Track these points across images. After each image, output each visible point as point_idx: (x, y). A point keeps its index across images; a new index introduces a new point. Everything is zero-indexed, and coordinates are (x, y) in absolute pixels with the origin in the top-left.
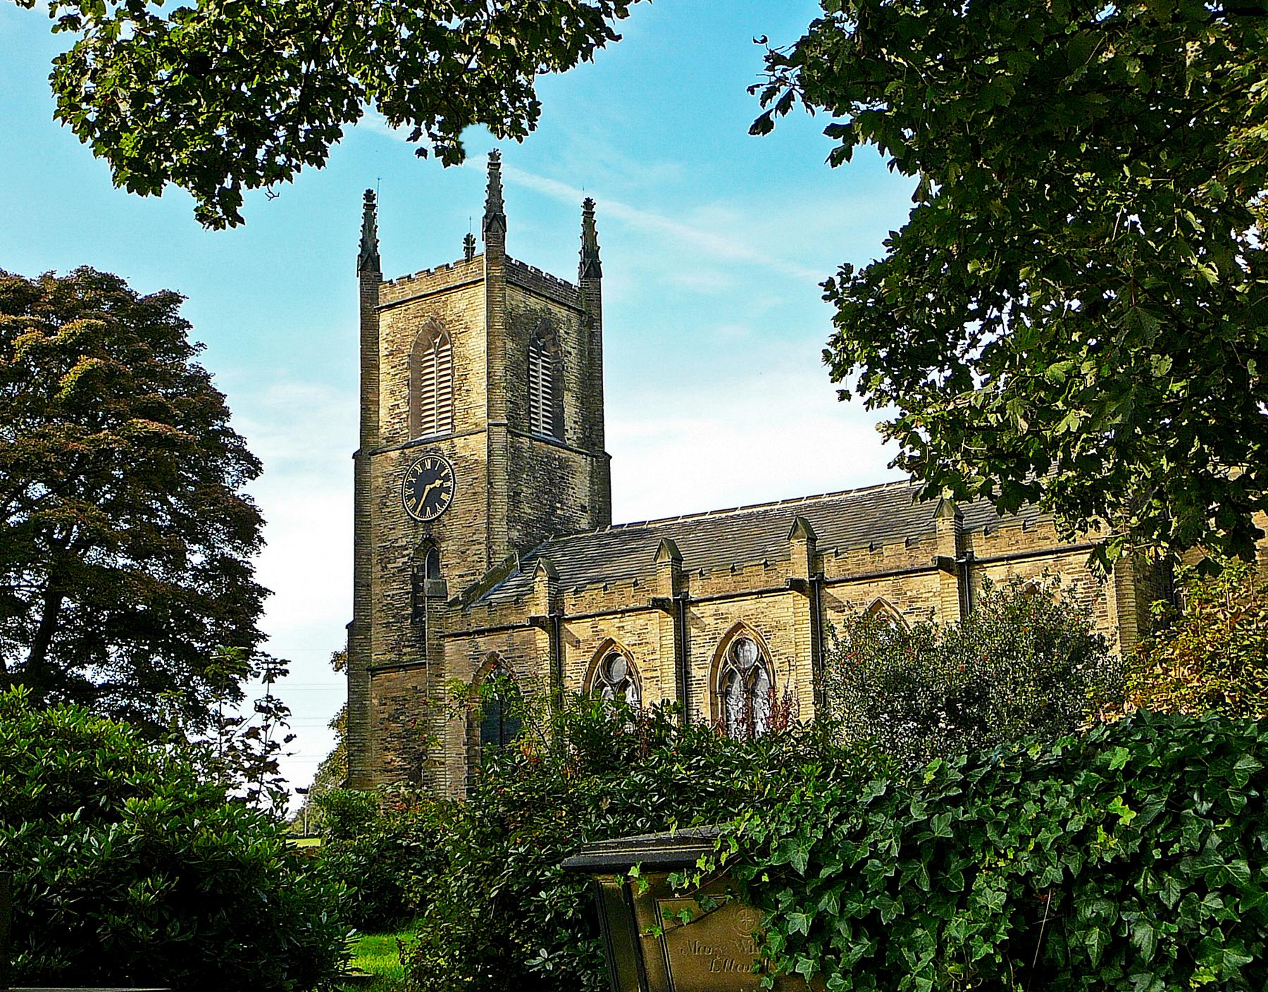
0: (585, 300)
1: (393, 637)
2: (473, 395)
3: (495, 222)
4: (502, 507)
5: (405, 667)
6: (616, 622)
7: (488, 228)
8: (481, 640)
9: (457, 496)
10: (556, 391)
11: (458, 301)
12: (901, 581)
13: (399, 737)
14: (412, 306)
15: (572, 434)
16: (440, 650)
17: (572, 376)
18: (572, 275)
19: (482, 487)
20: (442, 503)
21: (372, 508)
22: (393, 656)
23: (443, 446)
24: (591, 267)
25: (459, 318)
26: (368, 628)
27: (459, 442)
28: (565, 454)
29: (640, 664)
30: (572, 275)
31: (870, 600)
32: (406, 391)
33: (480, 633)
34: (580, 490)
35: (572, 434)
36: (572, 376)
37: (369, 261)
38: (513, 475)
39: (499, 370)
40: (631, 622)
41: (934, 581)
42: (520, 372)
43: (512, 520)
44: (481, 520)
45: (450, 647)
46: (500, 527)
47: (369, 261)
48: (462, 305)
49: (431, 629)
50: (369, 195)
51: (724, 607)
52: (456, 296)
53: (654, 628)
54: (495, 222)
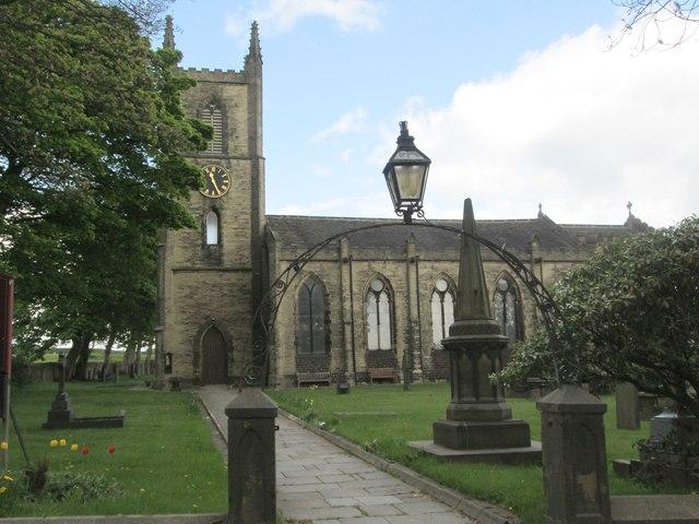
1: (189, 254)
2: (241, 139)
5: (198, 270)
13: (192, 306)
22: (185, 264)
23: (223, 161)
26: (172, 248)
27: (234, 162)
29: (394, 285)
44: (247, 203)
51: (436, 265)
52: (228, 87)
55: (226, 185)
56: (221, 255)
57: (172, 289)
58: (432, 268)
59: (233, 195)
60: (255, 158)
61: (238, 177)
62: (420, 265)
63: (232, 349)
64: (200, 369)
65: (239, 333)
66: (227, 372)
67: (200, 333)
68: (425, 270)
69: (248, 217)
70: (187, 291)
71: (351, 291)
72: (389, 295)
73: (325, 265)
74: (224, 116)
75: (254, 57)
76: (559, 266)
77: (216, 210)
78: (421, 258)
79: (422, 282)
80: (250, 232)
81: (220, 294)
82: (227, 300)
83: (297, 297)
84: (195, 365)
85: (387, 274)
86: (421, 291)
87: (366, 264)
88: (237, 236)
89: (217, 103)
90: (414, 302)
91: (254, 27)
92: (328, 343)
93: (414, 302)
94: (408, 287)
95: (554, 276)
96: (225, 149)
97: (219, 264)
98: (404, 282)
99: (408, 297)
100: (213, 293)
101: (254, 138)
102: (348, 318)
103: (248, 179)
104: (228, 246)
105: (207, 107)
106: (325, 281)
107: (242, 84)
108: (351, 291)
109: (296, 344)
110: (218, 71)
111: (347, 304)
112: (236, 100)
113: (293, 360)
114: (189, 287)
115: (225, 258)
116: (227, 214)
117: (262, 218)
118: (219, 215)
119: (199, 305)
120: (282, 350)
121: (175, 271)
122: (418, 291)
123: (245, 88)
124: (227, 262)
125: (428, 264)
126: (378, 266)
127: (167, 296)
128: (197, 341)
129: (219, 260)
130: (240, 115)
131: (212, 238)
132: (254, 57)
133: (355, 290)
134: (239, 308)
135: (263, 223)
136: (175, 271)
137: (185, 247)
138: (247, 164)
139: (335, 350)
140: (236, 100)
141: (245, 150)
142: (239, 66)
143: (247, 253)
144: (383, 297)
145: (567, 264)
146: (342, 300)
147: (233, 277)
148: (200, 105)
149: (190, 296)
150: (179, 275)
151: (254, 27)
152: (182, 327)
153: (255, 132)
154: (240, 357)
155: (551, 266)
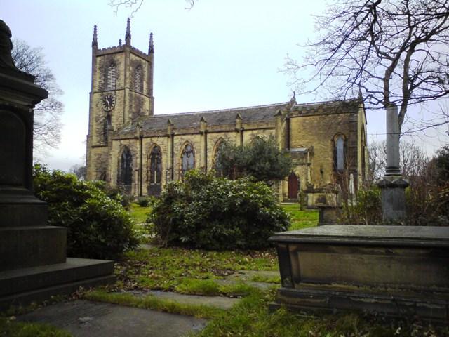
0: (149, 58)
1: (99, 139)
3: (128, 36)
4: (127, 108)
5: (102, 146)
6: (156, 139)
7: (126, 38)
8: (122, 141)
9: (116, 106)
10: (142, 81)
12: (227, 133)
14: (106, 56)
15: (145, 92)
16: (111, 143)
17: (146, 77)
18: (146, 51)
19: (122, 103)
21: (94, 106)
22: (98, 144)
23: (113, 92)
24: (151, 51)
25: (118, 60)
27: (117, 92)
28: (143, 96)
30: (146, 51)
31: (219, 137)
32: (103, 78)
34: (147, 105)
35: (145, 92)
36: (146, 77)
37: (95, 44)
38: (131, 101)
39: (128, 74)
40: (161, 139)
41: (234, 134)
42: (134, 75)
43: (130, 112)
44: (122, 111)
45: (114, 142)
46: (127, 113)
47: (95, 44)
49: (109, 138)
50: (95, 26)
51: (184, 137)
53: (166, 141)
54: (128, 36)
58: (181, 139)
61: (119, 99)
70: (97, 156)
73: (132, 141)
76: (255, 132)
79: (175, 146)
85: (159, 143)
86: (175, 152)
87: (149, 139)
95: (251, 139)
103: (122, 99)
105: (110, 66)
106: (131, 149)
107: (123, 52)
110: (104, 49)
119: (102, 163)
122: (173, 153)
123: (124, 53)
125: (179, 137)
126: (154, 140)
133: (144, 152)
141: (122, 85)
145: (260, 131)
149: (98, 159)
150: (95, 149)
155: (250, 132)
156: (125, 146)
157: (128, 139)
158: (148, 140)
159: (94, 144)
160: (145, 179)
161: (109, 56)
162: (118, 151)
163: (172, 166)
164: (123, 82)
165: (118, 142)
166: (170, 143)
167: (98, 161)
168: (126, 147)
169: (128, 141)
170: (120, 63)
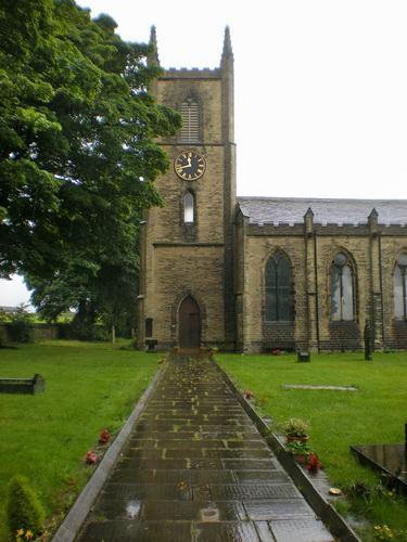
2: (214, 128)
5: (176, 245)
6: (345, 240)
8: (270, 240)
9: (207, 171)
11: (207, 86)
13: (170, 277)
20: (198, 174)
22: (165, 240)
23: (199, 148)
27: (208, 148)
29: (356, 258)
33: (270, 236)
40: (351, 241)
44: (221, 185)
48: (208, 88)
52: (204, 83)
55: (201, 169)
56: (197, 231)
57: (153, 261)
58: (395, 243)
59: (208, 177)
60: (227, 145)
61: (213, 161)
62: (382, 240)
63: (205, 316)
64: (177, 333)
65: (212, 303)
66: (200, 337)
67: (177, 301)
68: (388, 245)
69: (221, 197)
70: (167, 263)
71: (315, 264)
72: (352, 269)
74: (200, 108)
75: (227, 55)
77: (192, 191)
78: (383, 233)
79: (384, 256)
80: (221, 210)
81: (197, 268)
82: (201, 271)
83: (264, 269)
84: (173, 330)
86: (383, 264)
87: (330, 238)
88: (210, 214)
89: (194, 97)
90: (376, 275)
91: (227, 31)
92: (292, 313)
93: (376, 275)
94: (371, 265)
96: (201, 137)
97: (194, 240)
98: (366, 256)
99: (370, 271)
100: (189, 266)
101: (226, 126)
102: (312, 290)
103: (221, 163)
104: (203, 223)
105: (186, 101)
106: (290, 254)
107: (216, 79)
108: (315, 264)
109: (263, 313)
111: (311, 277)
112: (211, 93)
113: (259, 328)
114: (168, 260)
115: (200, 235)
116: (202, 195)
117: (233, 198)
118: (194, 195)
119: (176, 277)
120: (249, 319)
121: (156, 245)
122: (380, 265)
123: (218, 83)
124: (202, 238)
125: (391, 239)
126: (341, 241)
127: (148, 267)
128: (174, 308)
129: (195, 237)
130: (215, 106)
131: (189, 217)
132: (227, 55)
133: (319, 263)
134: (211, 279)
135: (234, 203)
136: (156, 245)
137: (165, 225)
138: (220, 150)
139: (299, 320)
140: (211, 93)
141: (218, 138)
142: (213, 63)
143: (220, 230)
144: (346, 270)
146: (307, 272)
147: (207, 252)
148: (179, 99)
149: (168, 268)
150: (159, 249)
151: (227, 31)
152: (162, 296)
153: (228, 121)
154: (213, 330)
156: (277, 247)
157: (284, 236)
158: (328, 241)
159: (157, 241)
160: (325, 310)
161: (186, 83)
162: (261, 257)
163: (381, 289)
164: (219, 132)
165: (262, 241)
166: (375, 250)
167: (168, 273)
168: (278, 250)
169: (283, 239)
170: (211, 98)
